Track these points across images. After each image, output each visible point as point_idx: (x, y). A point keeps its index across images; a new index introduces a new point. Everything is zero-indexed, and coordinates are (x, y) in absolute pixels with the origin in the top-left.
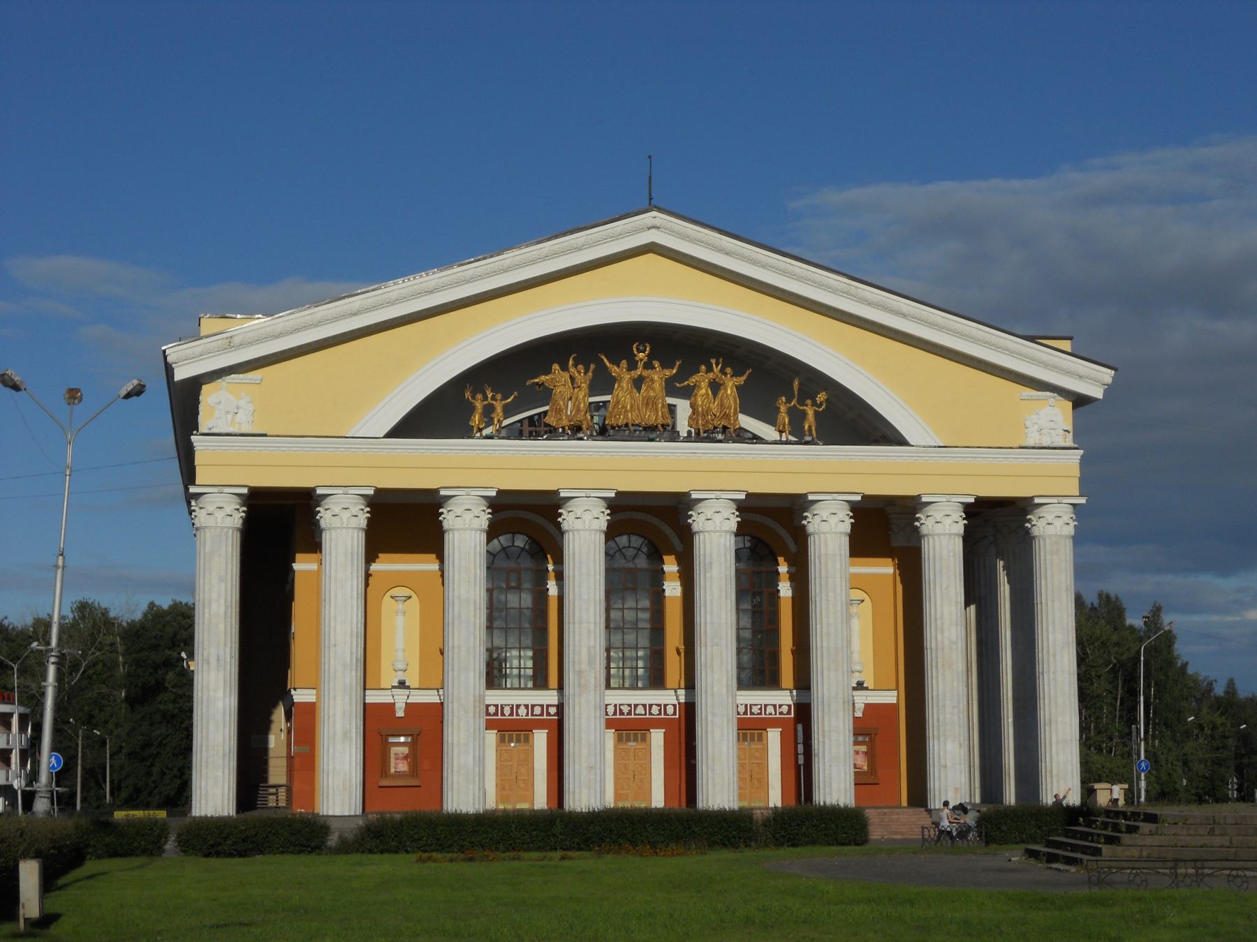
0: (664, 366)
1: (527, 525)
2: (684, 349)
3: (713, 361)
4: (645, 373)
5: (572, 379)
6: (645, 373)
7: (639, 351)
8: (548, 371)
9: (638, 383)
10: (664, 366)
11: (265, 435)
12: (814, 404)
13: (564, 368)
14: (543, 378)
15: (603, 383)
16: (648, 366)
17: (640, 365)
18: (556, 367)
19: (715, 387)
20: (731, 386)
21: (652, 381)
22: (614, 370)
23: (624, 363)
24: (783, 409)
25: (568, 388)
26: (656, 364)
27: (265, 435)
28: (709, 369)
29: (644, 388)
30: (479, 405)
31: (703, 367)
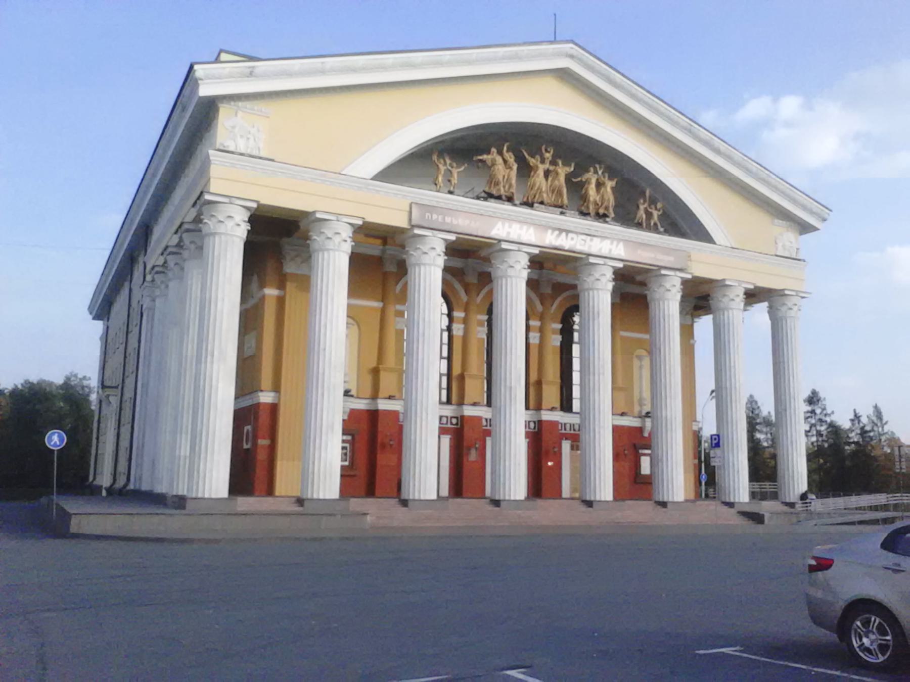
0: (566, 164)
1: (471, 265)
2: (579, 154)
3: (597, 166)
4: (552, 168)
5: (505, 161)
6: (552, 168)
7: (546, 151)
8: (489, 153)
9: (547, 174)
10: (564, 164)
11: (273, 160)
12: (656, 209)
13: (500, 153)
14: (485, 157)
15: (525, 170)
16: (553, 163)
17: (547, 162)
18: (494, 150)
19: (599, 185)
20: (610, 184)
21: (557, 174)
22: (532, 161)
23: (538, 157)
24: (642, 207)
25: (503, 167)
26: (560, 163)
27: (273, 160)
28: (596, 172)
29: (550, 179)
30: (442, 168)
31: (592, 169)
